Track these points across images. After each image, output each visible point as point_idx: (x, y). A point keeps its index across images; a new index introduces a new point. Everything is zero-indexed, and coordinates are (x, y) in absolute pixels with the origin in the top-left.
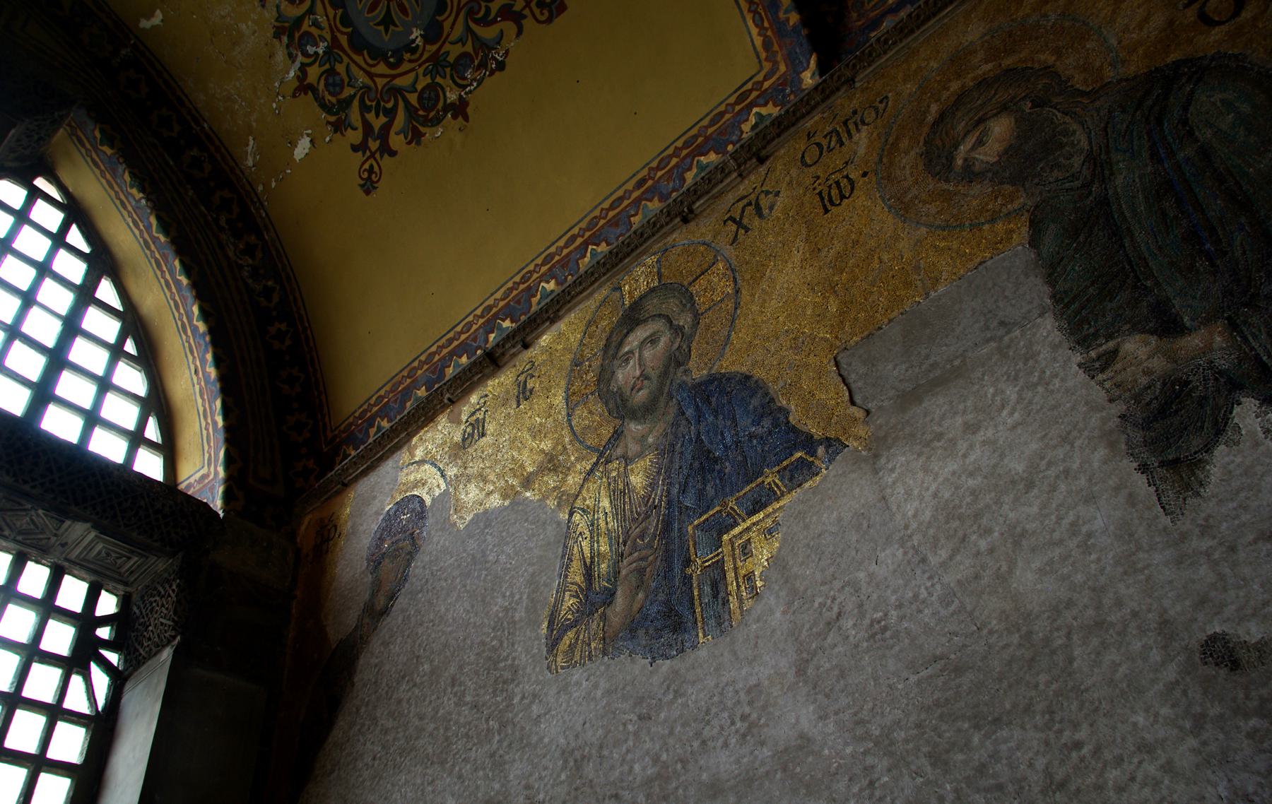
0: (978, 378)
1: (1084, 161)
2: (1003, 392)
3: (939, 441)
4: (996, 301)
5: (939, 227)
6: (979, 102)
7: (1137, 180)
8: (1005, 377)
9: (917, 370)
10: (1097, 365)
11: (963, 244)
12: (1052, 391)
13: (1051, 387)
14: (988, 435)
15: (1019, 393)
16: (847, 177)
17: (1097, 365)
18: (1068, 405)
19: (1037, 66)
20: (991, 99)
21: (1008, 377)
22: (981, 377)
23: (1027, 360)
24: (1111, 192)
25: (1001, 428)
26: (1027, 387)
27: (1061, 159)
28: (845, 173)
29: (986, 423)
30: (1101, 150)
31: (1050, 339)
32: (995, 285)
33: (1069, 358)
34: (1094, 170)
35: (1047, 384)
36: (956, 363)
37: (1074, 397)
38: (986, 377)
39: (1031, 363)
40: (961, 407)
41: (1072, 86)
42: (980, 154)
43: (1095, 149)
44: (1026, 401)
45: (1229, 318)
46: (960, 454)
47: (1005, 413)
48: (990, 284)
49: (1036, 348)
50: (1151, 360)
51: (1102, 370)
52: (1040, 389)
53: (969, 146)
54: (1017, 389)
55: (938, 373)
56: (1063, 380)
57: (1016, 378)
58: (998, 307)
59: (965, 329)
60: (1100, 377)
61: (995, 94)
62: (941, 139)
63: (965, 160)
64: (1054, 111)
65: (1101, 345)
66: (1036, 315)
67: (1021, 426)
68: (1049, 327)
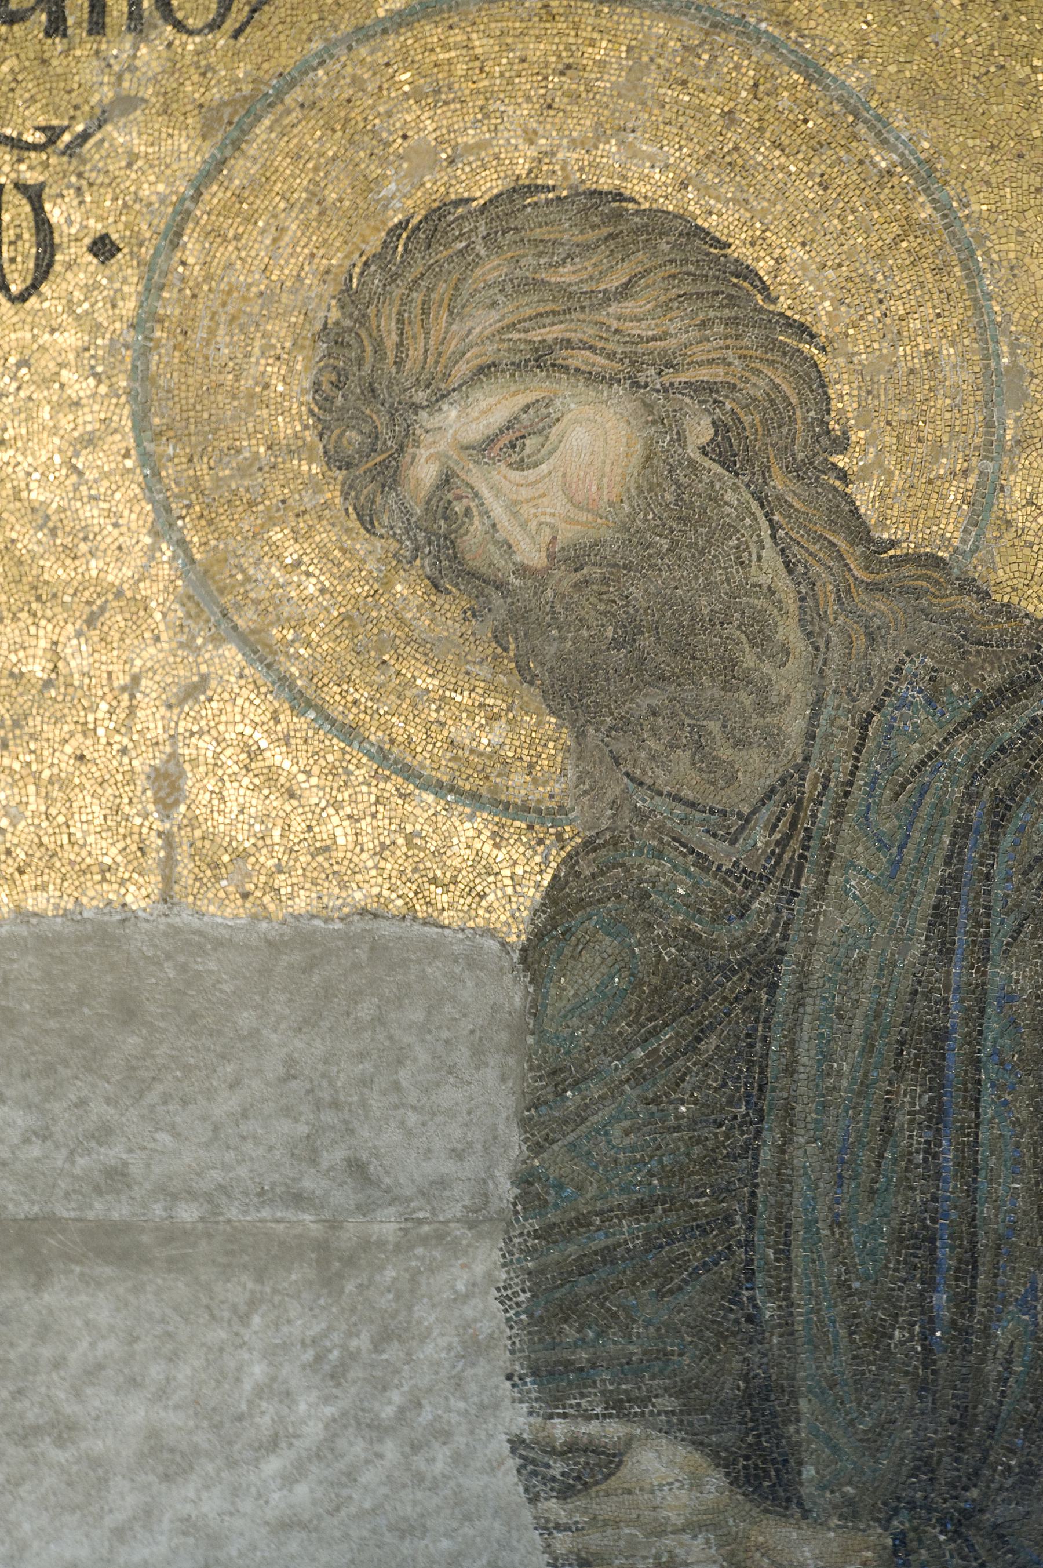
0: (234, 1309)
1: (773, 790)
2: (287, 1396)
3: (60, 1442)
4: (365, 1082)
5: (284, 681)
6: (566, 275)
7: (869, 964)
8: (309, 1355)
9: (59, 1159)
10: (557, 1468)
11: (337, 805)
12: (419, 1478)
13: (419, 1462)
14: (205, 1509)
15: (334, 1428)
16: (34, 196)
17: (557, 1468)
18: (445, 1544)
19: (784, 304)
20: (607, 298)
21: (319, 1358)
22: (243, 1308)
23: (383, 1339)
24: (795, 952)
25: (247, 1506)
26: (359, 1424)
27: (714, 726)
28: (32, 178)
29: (210, 1468)
30: (825, 787)
31: (469, 1312)
32: (380, 1020)
33: (496, 1406)
34: (783, 843)
35: (416, 1447)
36: (188, 1213)
37: (468, 1530)
38: (256, 1320)
39: (393, 1352)
40: (156, 1371)
41: (843, 476)
42: (498, 493)
43: (814, 770)
44: (341, 1465)
45: (901, 1540)
46: (109, 1521)
47: (273, 1465)
48: (365, 1010)
49: (425, 1315)
50: (686, 1537)
51: (565, 1493)
52: (390, 1449)
53: (476, 431)
54: (329, 1411)
55: (121, 1211)
56: (457, 1459)
57: (337, 1376)
58: (363, 1103)
59: (245, 1115)
60: (553, 1508)
61: (625, 291)
62: (400, 321)
63: (447, 480)
64: (764, 523)
65: (589, 1418)
66: (457, 1210)
67: (304, 1535)
68: (479, 1269)
